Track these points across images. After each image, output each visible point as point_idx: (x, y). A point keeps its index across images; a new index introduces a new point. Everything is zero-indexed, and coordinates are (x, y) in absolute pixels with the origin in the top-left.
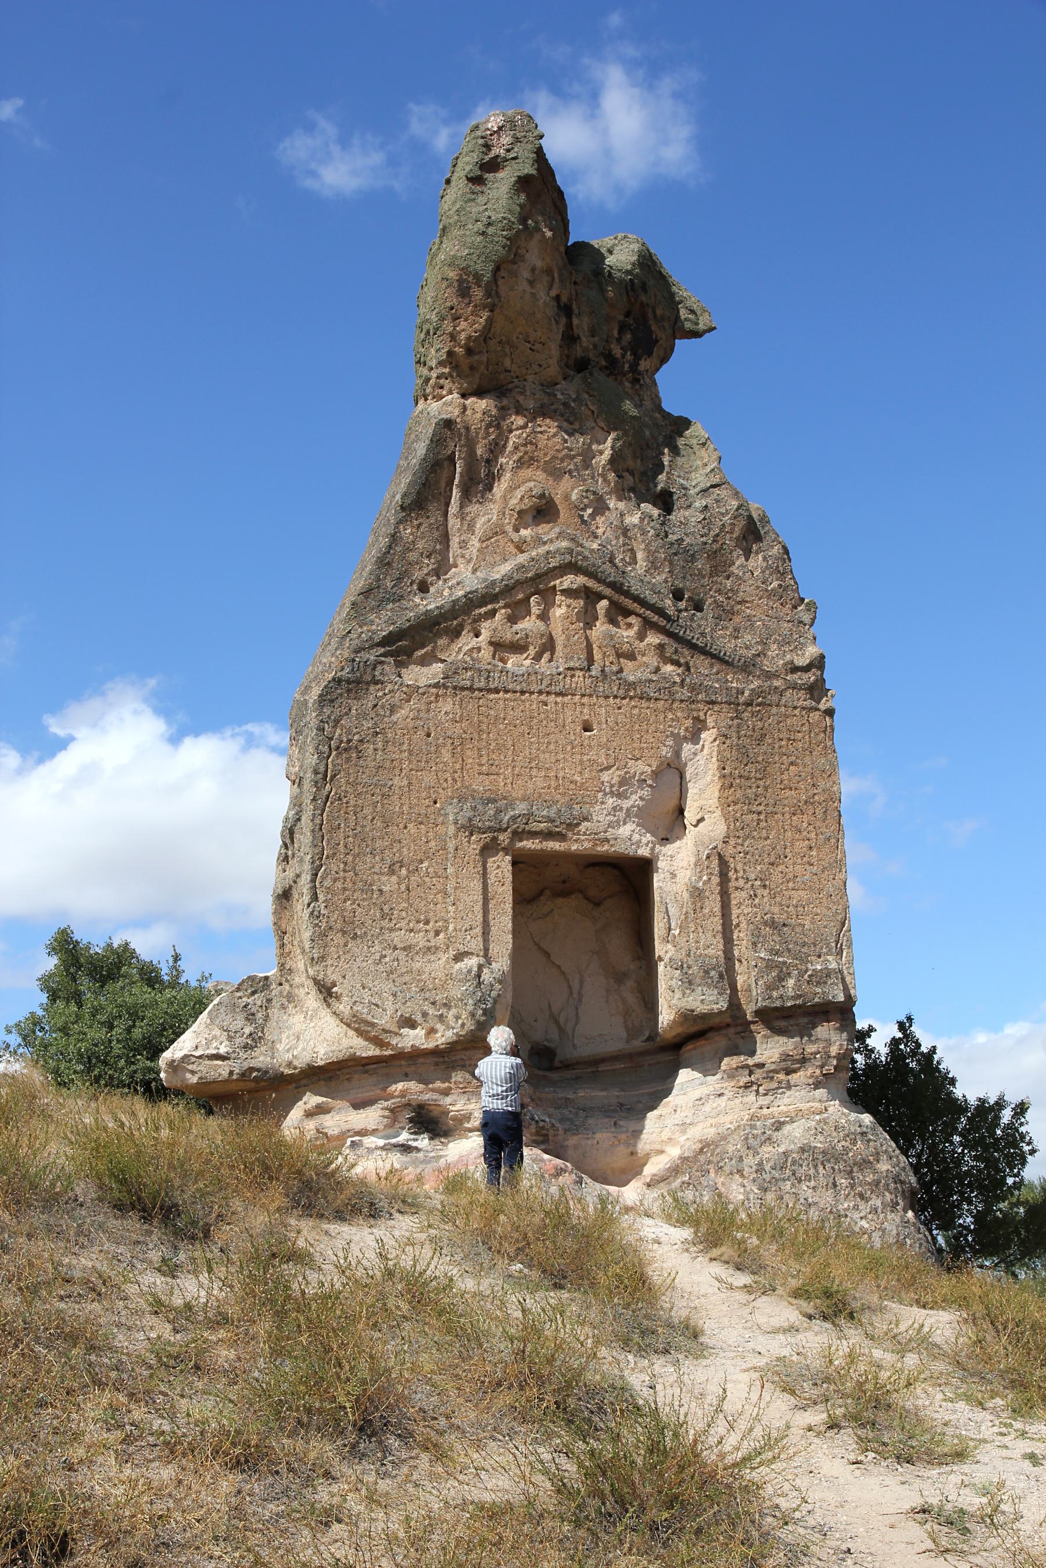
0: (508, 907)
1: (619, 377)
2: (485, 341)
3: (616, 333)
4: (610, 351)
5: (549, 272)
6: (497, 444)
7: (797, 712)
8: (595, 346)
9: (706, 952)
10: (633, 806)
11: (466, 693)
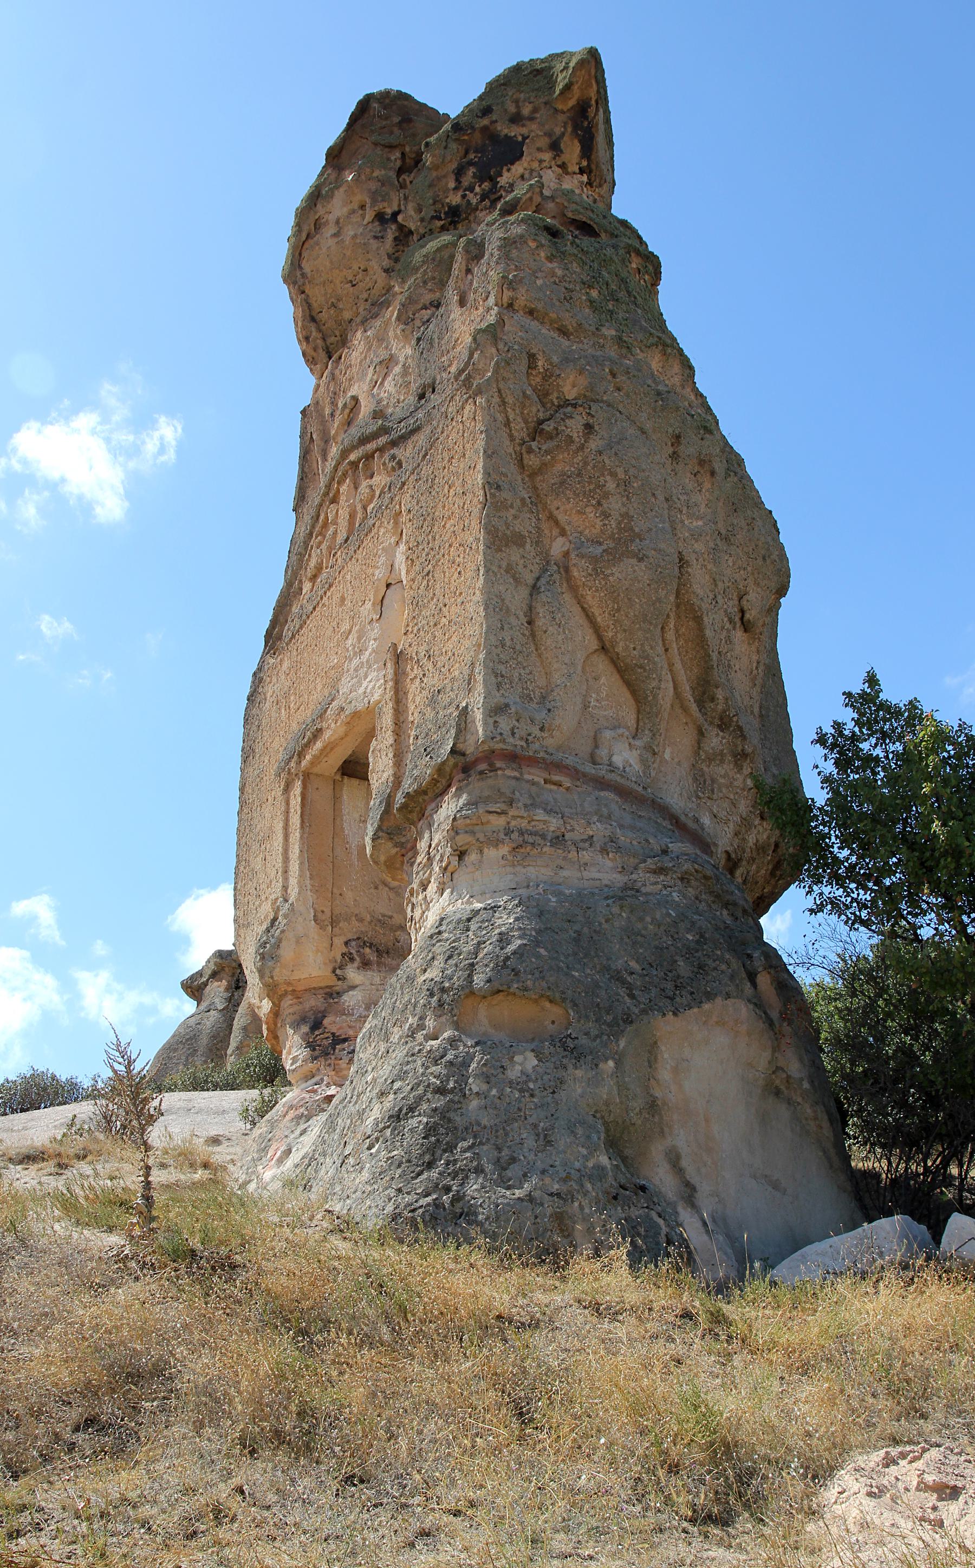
0: (298, 834)
1: (471, 218)
2: (313, 319)
3: (452, 185)
4: (450, 207)
5: (362, 207)
6: (335, 394)
8: (422, 220)
10: (370, 655)
11: (293, 641)
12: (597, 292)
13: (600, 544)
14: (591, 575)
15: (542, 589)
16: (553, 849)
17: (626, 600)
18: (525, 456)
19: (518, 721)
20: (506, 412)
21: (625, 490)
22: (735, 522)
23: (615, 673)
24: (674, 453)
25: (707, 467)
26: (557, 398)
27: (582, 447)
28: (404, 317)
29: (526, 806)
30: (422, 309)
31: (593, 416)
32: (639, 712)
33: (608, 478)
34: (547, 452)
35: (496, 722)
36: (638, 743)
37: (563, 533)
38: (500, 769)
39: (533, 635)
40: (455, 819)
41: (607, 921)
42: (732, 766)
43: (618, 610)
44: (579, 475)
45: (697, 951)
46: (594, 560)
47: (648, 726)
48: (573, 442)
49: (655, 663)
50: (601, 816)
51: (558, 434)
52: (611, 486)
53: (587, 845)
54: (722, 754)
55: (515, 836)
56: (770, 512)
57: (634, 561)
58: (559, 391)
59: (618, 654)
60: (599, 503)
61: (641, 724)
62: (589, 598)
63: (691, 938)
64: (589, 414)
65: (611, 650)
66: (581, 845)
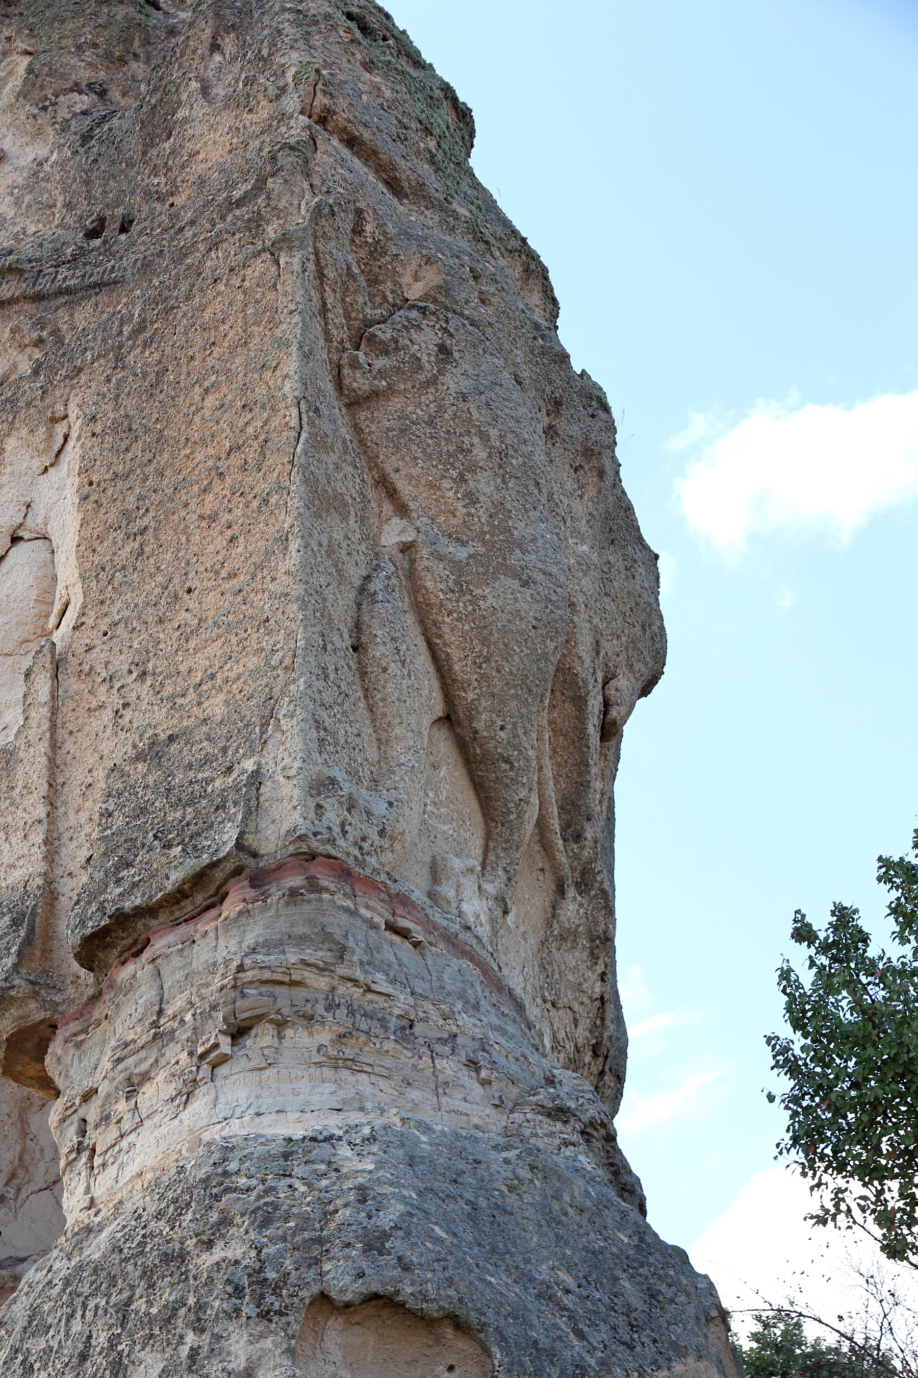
7: (221, 287)
9: (9, 881)
12: (435, 143)
13: (464, 544)
14: (452, 591)
15: (380, 597)
16: (399, 1047)
17: (501, 646)
18: (346, 371)
19: (349, 810)
20: (322, 292)
21: (500, 467)
22: (612, 559)
23: (460, 765)
24: (550, 427)
25: (594, 463)
26: (392, 292)
27: (432, 382)
28: (36, 94)
29: (361, 963)
30: (72, 90)
31: (451, 335)
32: (488, 837)
33: (476, 440)
34: (382, 374)
35: (319, 806)
36: (489, 887)
37: (402, 510)
38: (327, 890)
39: (363, 674)
40: (241, 968)
41: (511, 1189)
42: (586, 954)
43: (487, 660)
44: (430, 423)
45: (642, 1266)
46: (458, 567)
47: (503, 862)
48: (420, 368)
49: (527, 759)
50: (467, 1002)
51: (397, 349)
52: (480, 453)
53: (447, 1049)
54: (576, 934)
55: (342, 1013)
56: (657, 557)
57: (515, 584)
58: (395, 283)
59: (476, 732)
60: (462, 479)
61: (491, 857)
62: (446, 629)
63: (626, 1240)
64: (445, 330)
65: (466, 723)
66: (438, 1048)
